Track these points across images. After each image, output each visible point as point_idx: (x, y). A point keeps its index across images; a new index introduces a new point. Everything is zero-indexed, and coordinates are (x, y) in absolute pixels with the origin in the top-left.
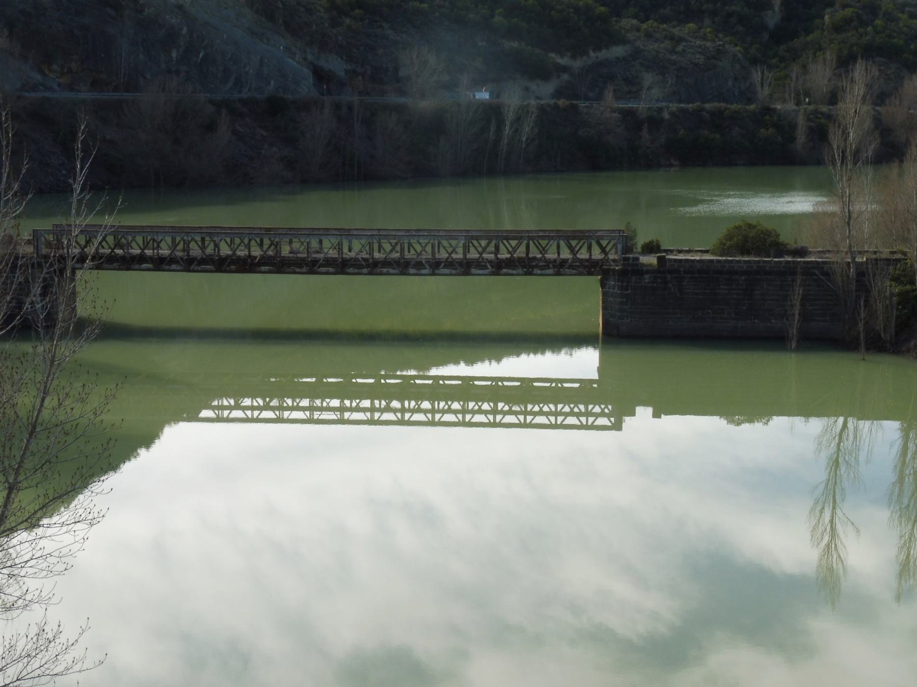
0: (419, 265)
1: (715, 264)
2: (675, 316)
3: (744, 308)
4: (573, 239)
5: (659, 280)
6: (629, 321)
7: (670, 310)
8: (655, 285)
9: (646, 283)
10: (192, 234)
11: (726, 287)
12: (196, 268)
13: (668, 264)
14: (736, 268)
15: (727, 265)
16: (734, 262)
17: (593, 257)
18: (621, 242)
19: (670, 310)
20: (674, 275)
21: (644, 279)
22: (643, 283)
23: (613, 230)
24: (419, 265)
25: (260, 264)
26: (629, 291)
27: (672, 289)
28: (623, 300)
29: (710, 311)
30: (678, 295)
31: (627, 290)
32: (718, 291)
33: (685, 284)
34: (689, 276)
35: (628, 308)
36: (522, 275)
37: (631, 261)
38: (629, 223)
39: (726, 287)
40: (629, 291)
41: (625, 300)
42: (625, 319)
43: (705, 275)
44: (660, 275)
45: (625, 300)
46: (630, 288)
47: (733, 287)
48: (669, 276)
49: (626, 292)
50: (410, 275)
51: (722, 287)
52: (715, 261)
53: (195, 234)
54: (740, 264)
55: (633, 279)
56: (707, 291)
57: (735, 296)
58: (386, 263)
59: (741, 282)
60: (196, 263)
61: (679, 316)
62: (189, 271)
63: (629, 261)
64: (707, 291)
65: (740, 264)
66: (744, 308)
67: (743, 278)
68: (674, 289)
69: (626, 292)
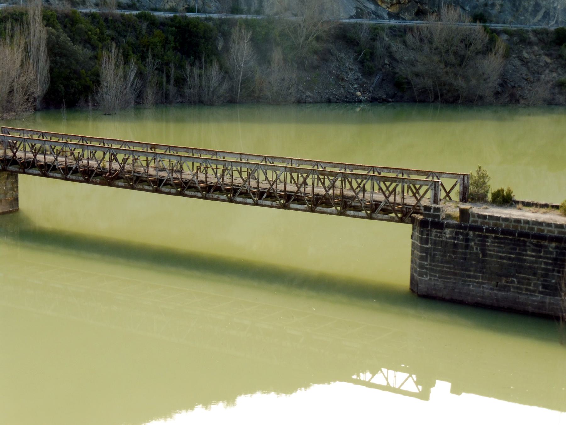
0: (245, 194)
1: (522, 225)
2: (477, 281)
3: (554, 281)
4: (388, 181)
5: (461, 237)
6: (427, 279)
7: (472, 273)
8: (456, 242)
9: (447, 238)
10: (69, 145)
11: (533, 254)
12: (72, 177)
13: (471, 219)
14: (545, 232)
15: (536, 227)
16: (544, 225)
17: (405, 201)
18: (434, 188)
19: (472, 273)
20: (477, 233)
21: (445, 233)
22: (443, 237)
23: (458, 174)
24: (245, 194)
25: (118, 178)
26: (429, 246)
27: (474, 249)
28: (422, 254)
29: (515, 279)
30: (481, 256)
31: (427, 244)
32: (524, 257)
33: (489, 244)
34: (493, 235)
35: (427, 265)
36: (336, 214)
37: (432, 211)
38: (480, 168)
39: (533, 254)
40: (429, 246)
41: (424, 254)
42: (424, 276)
43: (511, 237)
44: (461, 231)
45: (424, 254)
46: (430, 242)
47: (542, 254)
48: (471, 233)
49: (426, 246)
50: (236, 202)
51: (529, 253)
52: (522, 221)
53: (71, 145)
54: (550, 228)
55: (434, 232)
56: (513, 256)
57: (543, 266)
58: (218, 189)
59: (551, 249)
60: (71, 172)
61: (480, 280)
62: (66, 179)
63: (430, 211)
64: (513, 256)
65: (550, 228)
66: (554, 281)
67: (554, 245)
68: (477, 249)
69: (426, 246)
